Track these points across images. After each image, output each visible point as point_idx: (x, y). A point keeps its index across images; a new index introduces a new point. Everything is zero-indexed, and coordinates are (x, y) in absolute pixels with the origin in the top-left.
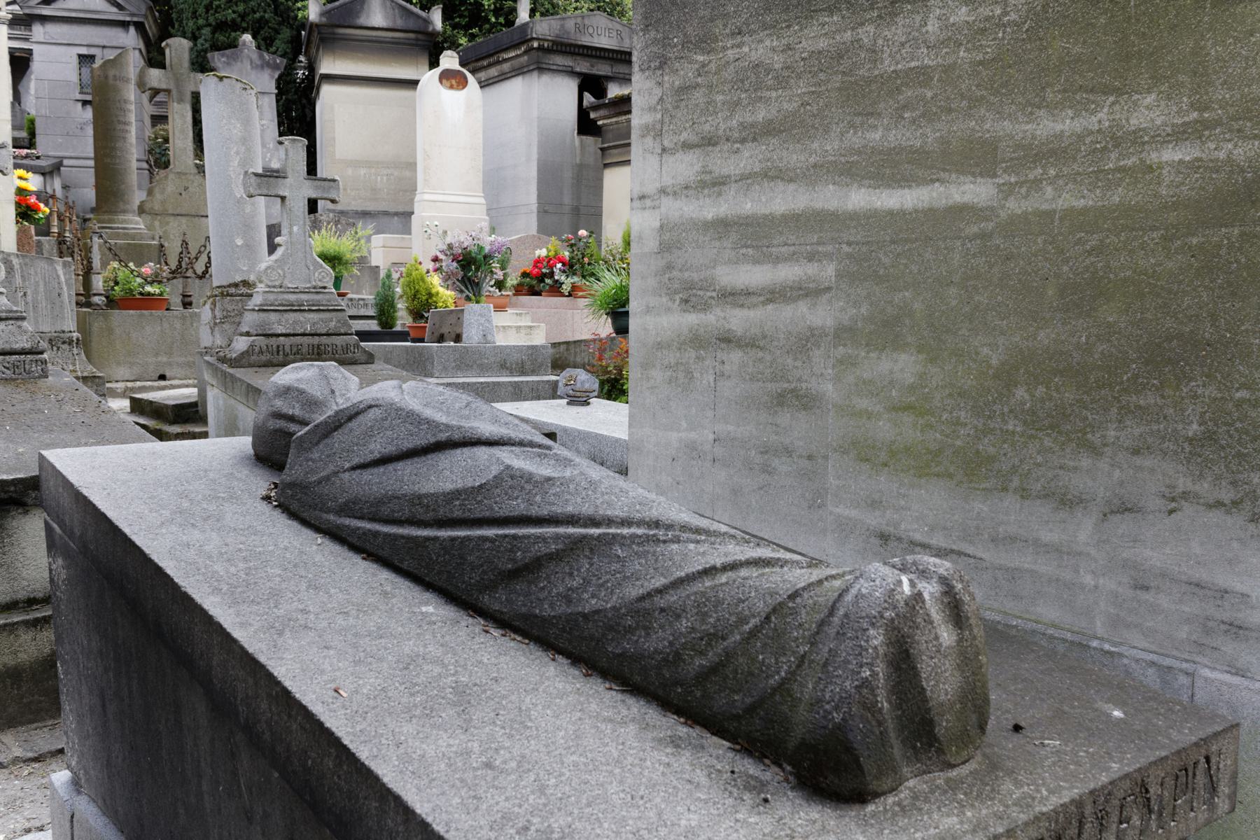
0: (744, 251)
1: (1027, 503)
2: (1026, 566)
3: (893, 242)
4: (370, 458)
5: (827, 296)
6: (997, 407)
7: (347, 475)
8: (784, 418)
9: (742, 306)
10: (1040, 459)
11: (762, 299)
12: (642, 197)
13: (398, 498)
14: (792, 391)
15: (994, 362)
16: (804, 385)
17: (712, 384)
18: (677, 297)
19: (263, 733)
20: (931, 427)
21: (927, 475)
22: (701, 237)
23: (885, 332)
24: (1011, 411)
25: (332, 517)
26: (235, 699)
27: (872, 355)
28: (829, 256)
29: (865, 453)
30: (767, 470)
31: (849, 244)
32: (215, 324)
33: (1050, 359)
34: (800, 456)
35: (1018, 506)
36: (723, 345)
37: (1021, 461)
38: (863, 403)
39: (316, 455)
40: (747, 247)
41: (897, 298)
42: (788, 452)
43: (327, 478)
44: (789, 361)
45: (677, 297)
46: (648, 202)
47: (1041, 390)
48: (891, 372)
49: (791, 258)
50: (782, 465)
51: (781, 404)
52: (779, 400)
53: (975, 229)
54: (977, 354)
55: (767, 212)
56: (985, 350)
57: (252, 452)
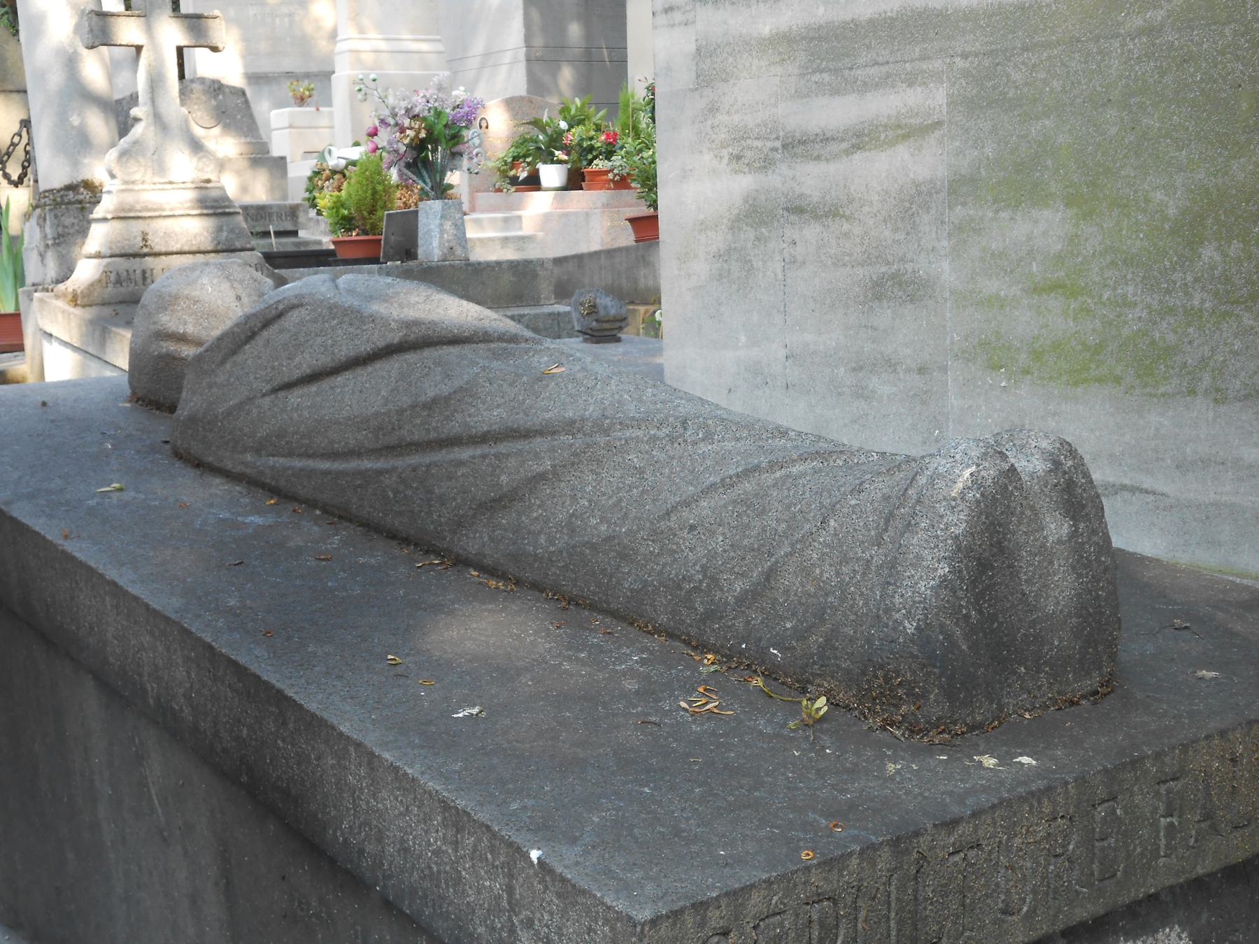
0: (817, 77)
1: (1223, 409)
2: (1224, 498)
3: (1025, 49)
4: (297, 374)
5: (937, 134)
6: (1177, 276)
7: (267, 401)
8: (884, 316)
9: (818, 158)
10: (1237, 345)
11: (844, 146)
12: (669, 10)
13: (337, 423)
14: (893, 277)
15: (1172, 211)
16: (909, 267)
17: (780, 276)
18: (725, 153)
19: (181, 710)
20: (1088, 311)
21: (1085, 381)
22: (756, 61)
23: (1018, 183)
24: (1196, 280)
25: (248, 457)
26: (140, 675)
27: (1003, 215)
28: (936, 76)
29: (992, 354)
30: (860, 393)
31: (965, 56)
32: (47, 246)
33: (1248, 202)
34: (908, 370)
35: (1211, 414)
36: (793, 218)
37: (1213, 350)
38: (991, 286)
39: (221, 378)
40: (822, 71)
41: (1035, 129)
42: (891, 365)
43: (240, 406)
44: (887, 233)
45: (725, 153)
46: (678, 16)
47: (1235, 248)
48: (1029, 238)
49: (885, 82)
50: (881, 385)
51: (878, 297)
52: (877, 291)
53: (1138, 22)
54: (1147, 201)
55: (848, 17)
56: (1159, 196)
57: (128, 392)
